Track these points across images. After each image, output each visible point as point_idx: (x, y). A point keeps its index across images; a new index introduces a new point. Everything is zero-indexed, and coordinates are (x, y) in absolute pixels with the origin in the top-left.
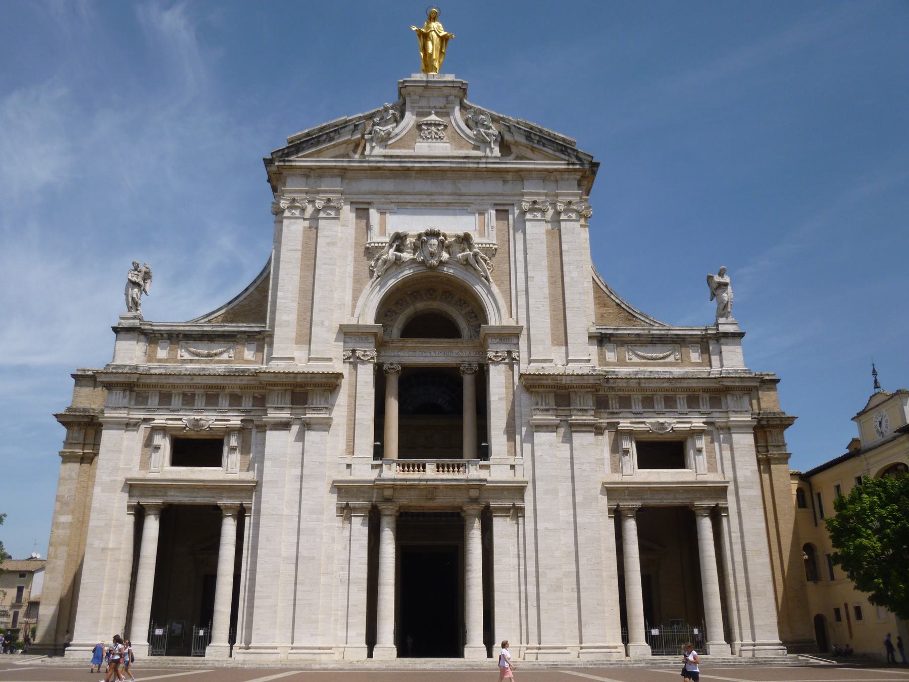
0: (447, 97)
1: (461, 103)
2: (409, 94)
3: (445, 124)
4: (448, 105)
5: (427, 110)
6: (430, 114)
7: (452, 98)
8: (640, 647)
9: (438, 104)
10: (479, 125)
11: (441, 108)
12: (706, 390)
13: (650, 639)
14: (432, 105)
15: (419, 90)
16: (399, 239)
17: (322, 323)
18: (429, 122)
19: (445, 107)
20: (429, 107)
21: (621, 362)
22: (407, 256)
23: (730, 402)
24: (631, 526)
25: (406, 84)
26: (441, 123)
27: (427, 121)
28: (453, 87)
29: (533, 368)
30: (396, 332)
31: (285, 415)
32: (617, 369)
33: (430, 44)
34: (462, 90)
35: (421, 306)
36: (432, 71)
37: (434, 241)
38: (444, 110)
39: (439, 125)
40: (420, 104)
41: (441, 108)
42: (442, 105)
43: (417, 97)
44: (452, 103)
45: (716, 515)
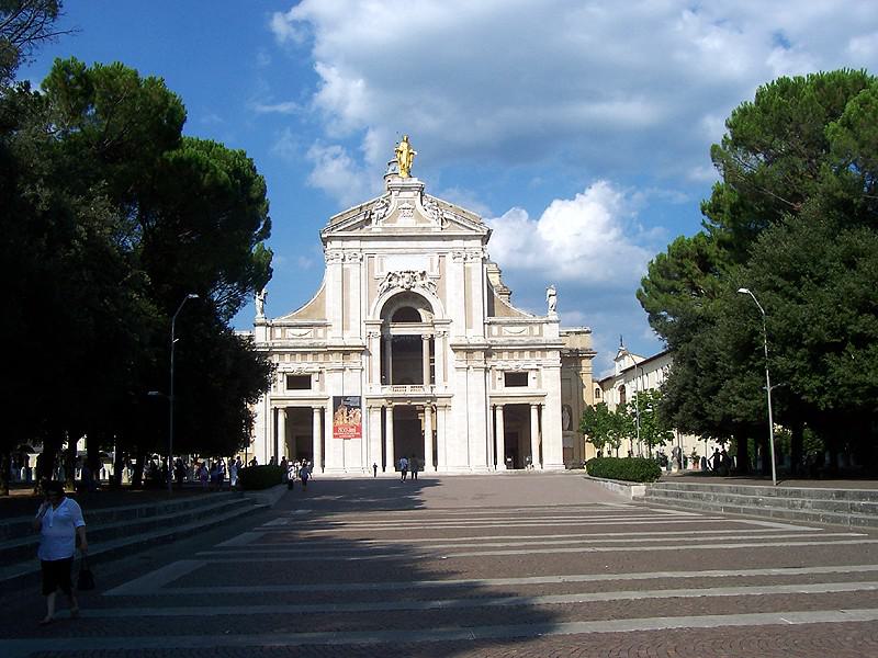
8: (502, 467)
12: (539, 349)
13: (505, 460)
16: (392, 276)
17: (354, 320)
21: (498, 336)
22: (394, 282)
23: (549, 354)
24: (499, 414)
29: (456, 343)
30: (390, 319)
31: (340, 366)
32: (497, 339)
35: (402, 304)
37: (407, 275)
45: (540, 408)
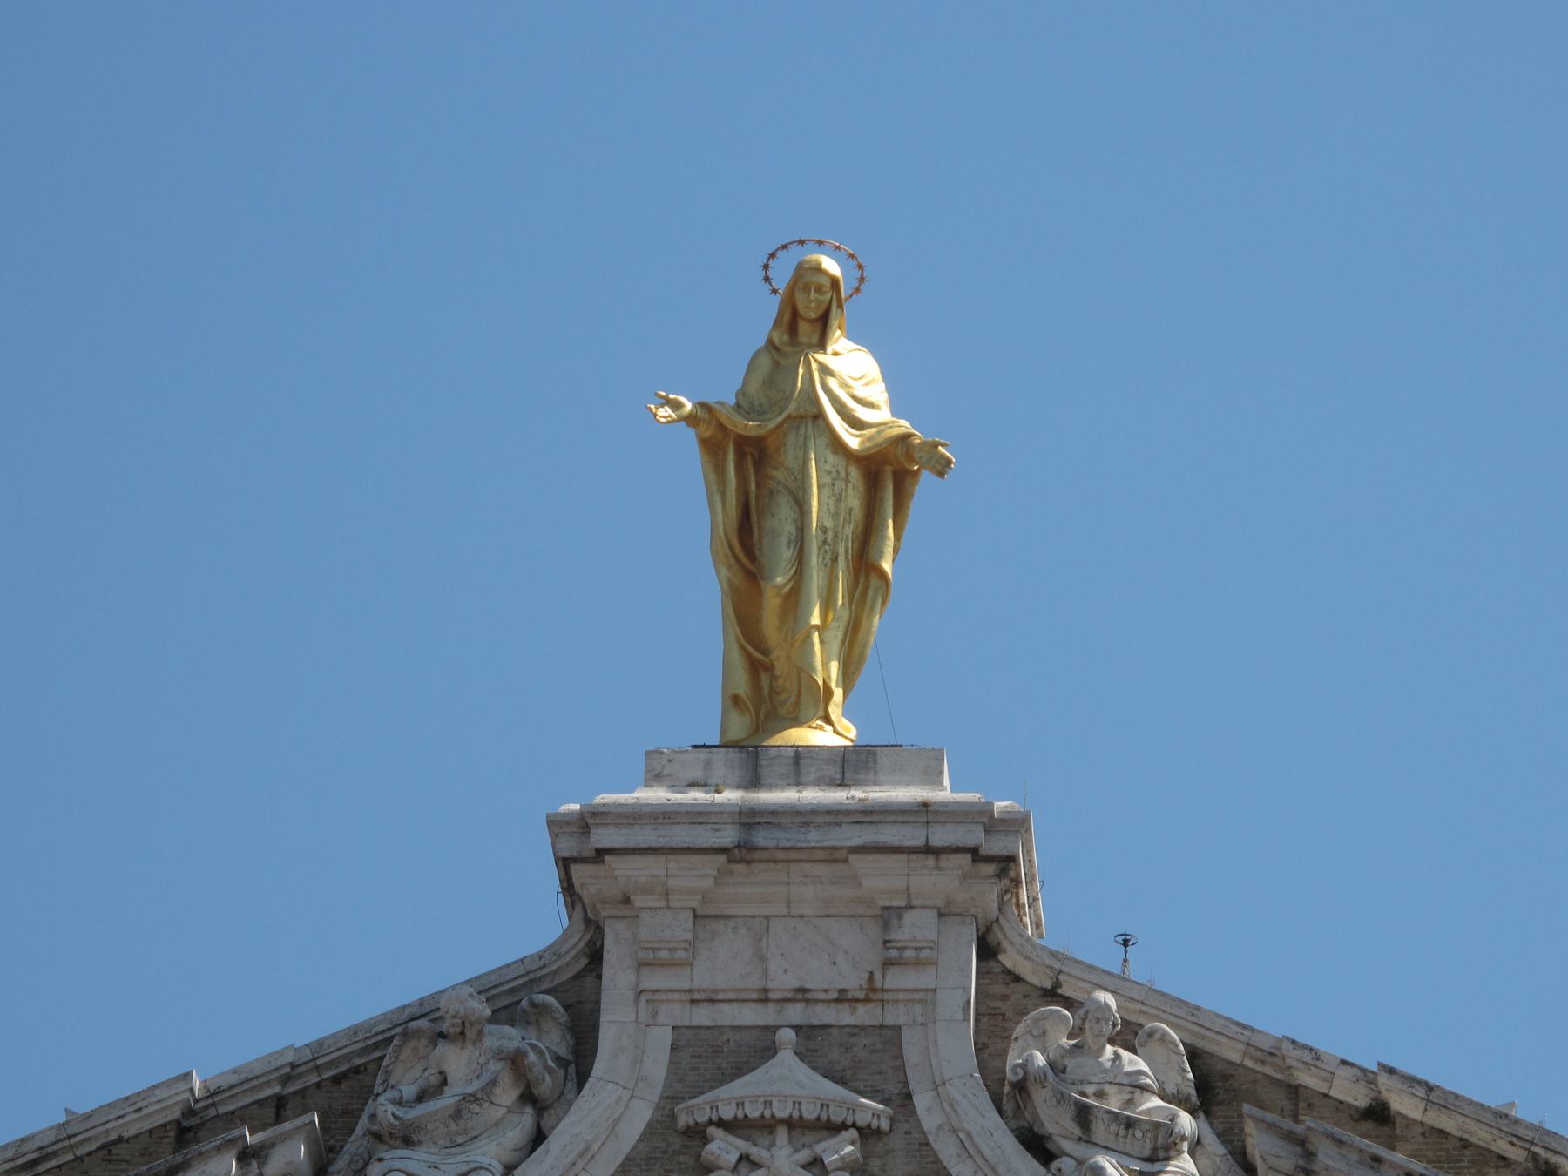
0: (888, 917)
1: (987, 951)
2: (627, 900)
3: (863, 1119)
4: (896, 979)
5: (750, 1015)
6: (762, 1048)
7: (917, 927)
9: (820, 976)
10: (1100, 1131)
11: (842, 998)
14: (783, 980)
15: (694, 877)
18: (754, 1112)
19: (872, 993)
20: (764, 998)
25: (604, 837)
26: (837, 1116)
27: (740, 1104)
28: (928, 850)
33: (782, 518)
34: (990, 869)
36: (796, 722)
38: (864, 1015)
39: (835, 1128)
40: (702, 976)
41: (842, 998)
42: (853, 981)
43: (679, 928)
44: (918, 963)
